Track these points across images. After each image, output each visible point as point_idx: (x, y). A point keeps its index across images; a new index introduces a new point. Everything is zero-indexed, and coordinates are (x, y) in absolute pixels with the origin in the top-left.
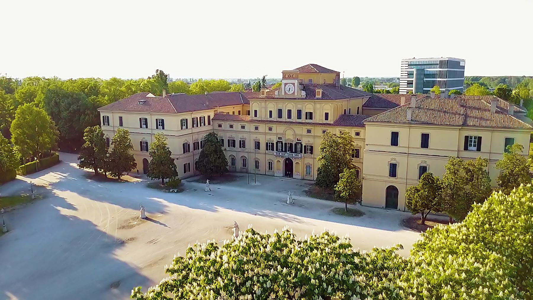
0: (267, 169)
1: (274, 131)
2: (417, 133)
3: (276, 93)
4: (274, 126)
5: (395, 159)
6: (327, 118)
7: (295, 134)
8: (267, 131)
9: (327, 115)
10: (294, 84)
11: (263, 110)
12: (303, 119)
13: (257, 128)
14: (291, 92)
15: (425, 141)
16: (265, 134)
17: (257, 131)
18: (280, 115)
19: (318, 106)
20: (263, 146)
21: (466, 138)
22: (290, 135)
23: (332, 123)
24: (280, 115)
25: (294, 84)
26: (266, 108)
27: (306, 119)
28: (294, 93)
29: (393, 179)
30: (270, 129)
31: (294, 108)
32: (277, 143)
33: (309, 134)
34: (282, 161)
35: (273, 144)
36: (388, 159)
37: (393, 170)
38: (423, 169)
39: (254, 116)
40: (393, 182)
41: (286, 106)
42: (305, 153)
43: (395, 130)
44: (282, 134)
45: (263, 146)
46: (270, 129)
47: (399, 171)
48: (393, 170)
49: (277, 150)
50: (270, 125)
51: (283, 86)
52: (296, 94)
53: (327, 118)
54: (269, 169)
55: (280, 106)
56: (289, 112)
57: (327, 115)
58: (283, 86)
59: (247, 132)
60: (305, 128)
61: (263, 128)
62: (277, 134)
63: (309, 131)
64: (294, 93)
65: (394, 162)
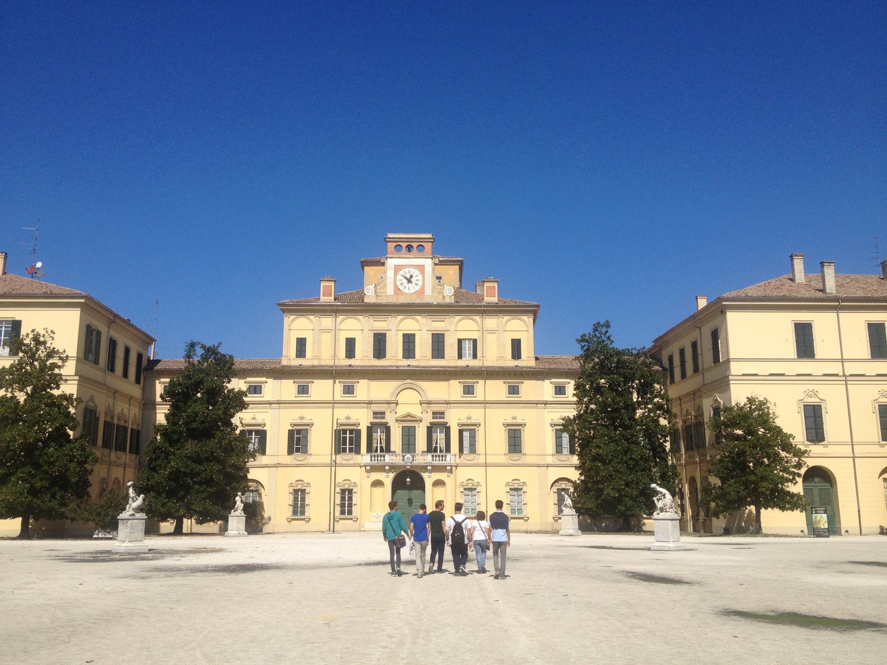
5: (815, 393)
6: (516, 351)
8: (339, 395)
9: (516, 345)
10: (421, 268)
11: (327, 338)
14: (412, 288)
16: (333, 403)
18: (380, 349)
19: (491, 322)
23: (532, 363)
24: (380, 349)
25: (421, 268)
26: (335, 331)
27: (460, 356)
28: (421, 292)
30: (349, 390)
32: (370, 430)
33: (469, 398)
34: (388, 479)
35: (359, 432)
43: (803, 317)
46: (349, 390)
49: (369, 449)
51: (390, 273)
52: (428, 291)
53: (516, 351)
56: (409, 341)
57: (516, 345)
58: (390, 273)
61: (321, 389)
62: (370, 403)
64: (421, 292)
65: (813, 400)
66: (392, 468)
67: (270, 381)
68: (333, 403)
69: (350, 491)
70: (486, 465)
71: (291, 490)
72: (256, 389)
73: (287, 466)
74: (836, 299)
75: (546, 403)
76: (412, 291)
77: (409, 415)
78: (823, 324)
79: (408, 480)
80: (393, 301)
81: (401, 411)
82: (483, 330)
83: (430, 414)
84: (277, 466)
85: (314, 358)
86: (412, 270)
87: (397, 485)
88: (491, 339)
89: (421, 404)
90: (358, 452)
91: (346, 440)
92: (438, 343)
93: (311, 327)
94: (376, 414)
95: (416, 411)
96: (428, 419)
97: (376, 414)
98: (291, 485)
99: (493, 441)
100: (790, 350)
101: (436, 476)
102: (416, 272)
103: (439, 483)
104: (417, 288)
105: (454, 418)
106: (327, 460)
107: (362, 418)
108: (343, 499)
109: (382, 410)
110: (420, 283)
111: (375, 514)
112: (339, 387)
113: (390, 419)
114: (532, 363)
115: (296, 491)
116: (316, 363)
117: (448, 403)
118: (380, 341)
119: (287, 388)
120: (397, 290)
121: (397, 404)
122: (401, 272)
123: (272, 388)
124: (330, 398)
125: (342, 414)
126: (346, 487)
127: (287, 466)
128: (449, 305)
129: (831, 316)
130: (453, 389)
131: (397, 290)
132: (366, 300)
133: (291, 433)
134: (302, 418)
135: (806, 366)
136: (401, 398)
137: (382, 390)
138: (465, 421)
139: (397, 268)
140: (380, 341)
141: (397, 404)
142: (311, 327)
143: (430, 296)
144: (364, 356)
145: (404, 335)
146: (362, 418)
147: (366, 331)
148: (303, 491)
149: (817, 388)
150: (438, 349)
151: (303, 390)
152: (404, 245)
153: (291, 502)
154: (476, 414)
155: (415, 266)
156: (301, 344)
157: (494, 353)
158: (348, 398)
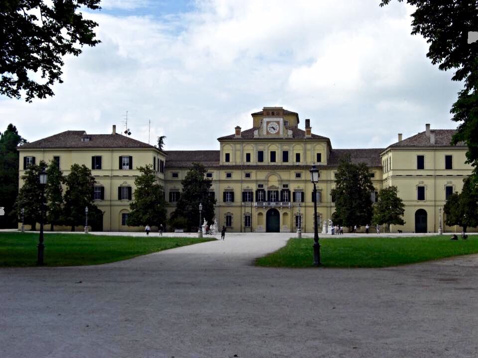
0: (243, 225)
1: (253, 177)
2: (441, 156)
3: (256, 133)
6: (319, 159)
7: (281, 181)
8: (244, 178)
9: (319, 156)
10: (278, 123)
13: (229, 175)
14: (274, 132)
17: (229, 179)
19: (309, 146)
20: (238, 197)
22: (274, 182)
23: (325, 164)
25: (278, 123)
26: (243, 150)
28: (278, 133)
29: (421, 203)
30: (248, 175)
31: (279, 150)
32: (257, 192)
33: (298, 179)
34: (265, 212)
36: (416, 182)
37: (421, 192)
38: (449, 190)
39: (225, 161)
40: (421, 205)
42: (294, 200)
43: (421, 153)
44: (264, 181)
45: (238, 197)
46: (248, 175)
47: (428, 194)
48: (421, 192)
49: (257, 201)
50: (248, 171)
52: (281, 133)
54: (246, 225)
55: (261, 148)
57: (319, 156)
59: (215, 181)
61: (237, 175)
62: (257, 181)
63: (298, 175)
64: (278, 133)
65: (422, 185)
66: (266, 207)
67: (215, 171)
68: (242, 181)
69: (249, 217)
70: (305, 207)
71: (225, 216)
72: (210, 175)
73: (224, 206)
74: (433, 146)
75: (331, 181)
76: (274, 132)
77: (273, 186)
79: (273, 213)
80: (267, 137)
81: (270, 184)
82: (305, 150)
83: (282, 186)
84: (220, 206)
85: (232, 162)
86: (274, 123)
87: (268, 214)
88: (309, 153)
89: (279, 181)
90: (252, 200)
91: (247, 196)
92: (285, 156)
93: (231, 149)
94: (259, 186)
95: (276, 184)
96: (280, 188)
97: (259, 186)
98: (225, 214)
100: (415, 166)
101: (285, 211)
102: (275, 125)
103: (285, 214)
104: (277, 131)
105: (292, 187)
106: (239, 204)
107: (254, 187)
108: (246, 220)
109: (262, 184)
110: (278, 129)
111: (259, 226)
112: (244, 175)
113: (266, 188)
114: (325, 164)
115: (227, 217)
116: (234, 164)
117: (289, 181)
118: (261, 156)
119: (222, 175)
120: (268, 133)
121: (268, 181)
122: (270, 124)
123: (217, 175)
124: (240, 179)
126: (248, 215)
127: (224, 206)
128: (290, 139)
130: (292, 175)
131: (268, 133)
132: (255, 137)
133: (224, 193)
134: (229, 187)
135: (420, 172)
136: (270, 179)
137: (261, 175)
138: (297, 189)
139: (268, 123)
140: (261, 156)
141: (268, 181)
142: (231, 149)
143: (282, 135)
145: (271, 152)
146: (254, 187)
147: (255, 150)
148: (230, 217)
149: (423, 180)
151: (229, 175)
152: (271, 112)
153: (225, 221)
154: (302, 186)
155: (275, 122)
156: (228, 156)
157: (311, 160)
158: (248, 179)
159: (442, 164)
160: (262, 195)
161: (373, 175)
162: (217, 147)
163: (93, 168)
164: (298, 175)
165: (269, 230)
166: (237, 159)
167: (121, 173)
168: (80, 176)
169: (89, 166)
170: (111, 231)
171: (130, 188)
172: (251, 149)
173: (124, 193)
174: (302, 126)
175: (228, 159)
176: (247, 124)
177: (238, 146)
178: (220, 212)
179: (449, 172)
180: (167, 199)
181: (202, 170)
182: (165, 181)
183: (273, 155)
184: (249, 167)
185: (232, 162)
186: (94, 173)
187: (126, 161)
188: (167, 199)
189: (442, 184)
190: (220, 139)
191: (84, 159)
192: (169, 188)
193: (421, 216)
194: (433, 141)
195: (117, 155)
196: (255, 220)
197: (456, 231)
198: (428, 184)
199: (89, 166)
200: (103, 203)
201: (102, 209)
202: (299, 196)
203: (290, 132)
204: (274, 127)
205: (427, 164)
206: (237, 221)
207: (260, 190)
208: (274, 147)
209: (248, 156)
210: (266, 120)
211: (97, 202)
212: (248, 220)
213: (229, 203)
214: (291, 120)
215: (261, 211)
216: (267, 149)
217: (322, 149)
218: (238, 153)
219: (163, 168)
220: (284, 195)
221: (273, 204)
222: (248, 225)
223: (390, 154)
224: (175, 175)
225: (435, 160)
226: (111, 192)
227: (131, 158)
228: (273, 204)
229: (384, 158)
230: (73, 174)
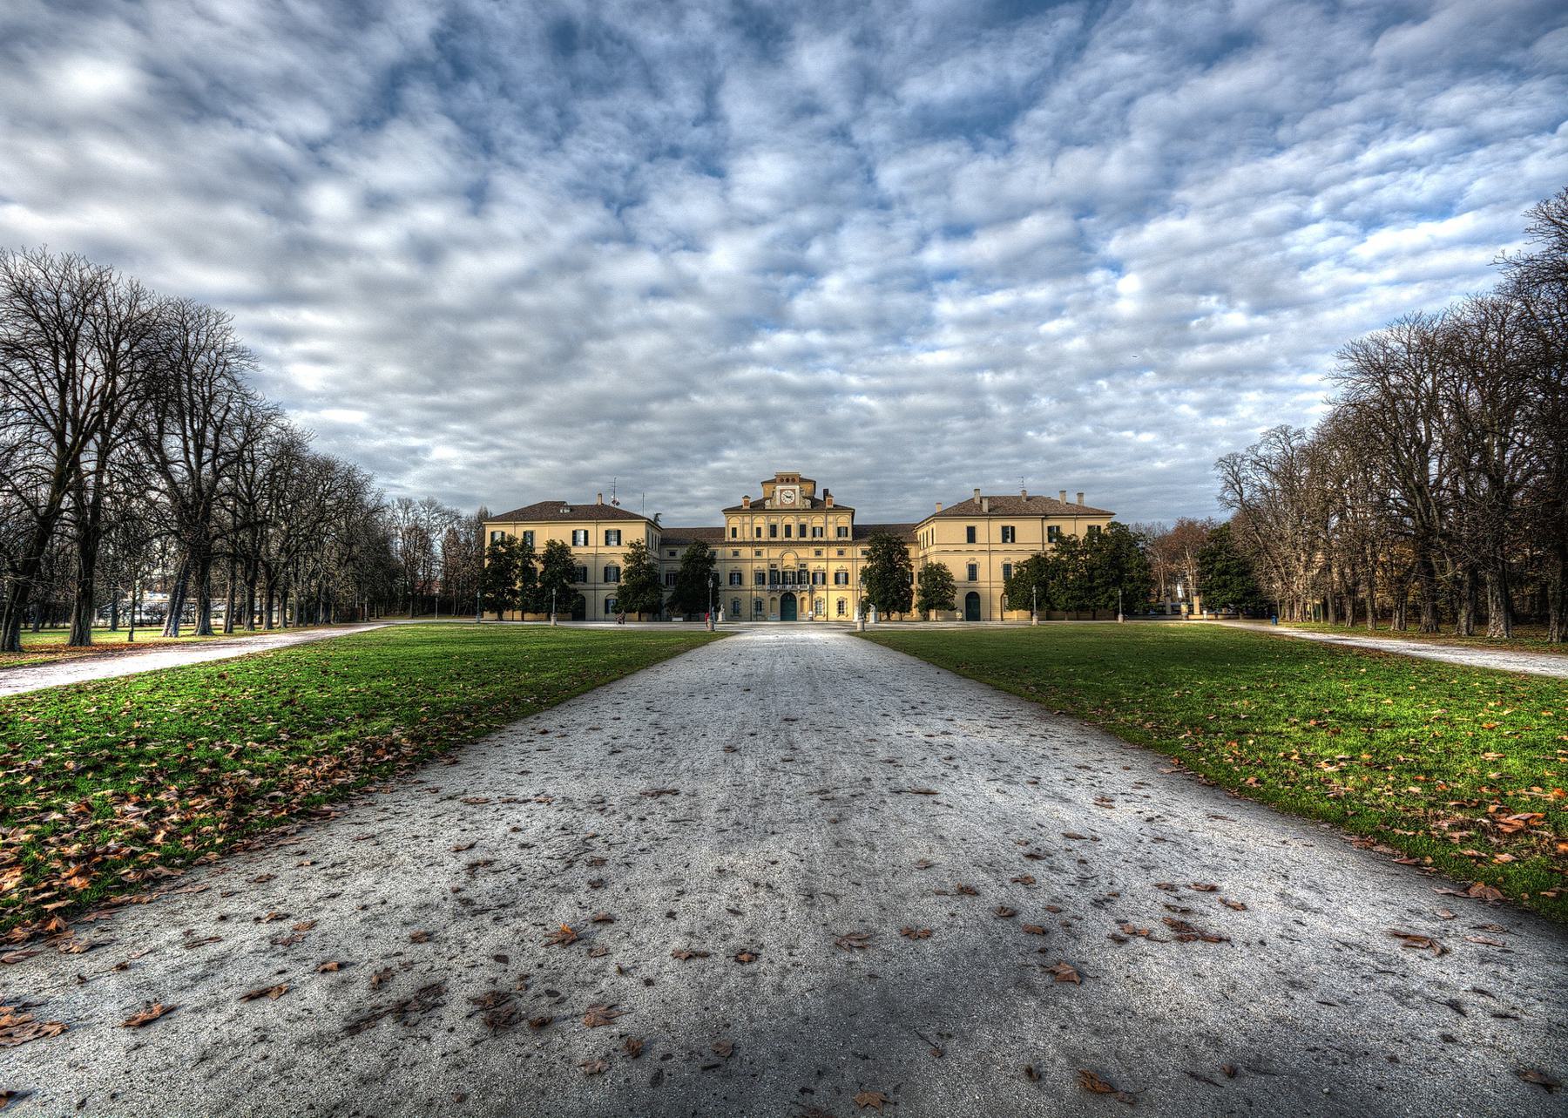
1: (765, 556)
3: (768, 503)
4: (765, 550)
12: (808, 538)
14: (789, 501)
15: (1008, 534)
18: (774, 534)
19: (831, 518)
21: (1050, 529)
22: (788, 561)
24: (774, 534)
30: (758, 553)
37: (973, 569)
38: (1007, 568)
41: (781, 521)
43: (971, 524)
46: (758, 553)
47: (982, 574)
48: (973, 569)
55: (774, 520)
60: (812, 550)
61: (746, 552)
63: (818, 553)
78: (981, 527)
92: (803, 529)
95: (793, 564)
99: (831, 579)
105: (812, 567)
125: (756, 566)
129: (985, 523)
137: (775, 553)
144: (765, 536)
146: (764, 566)
150: (803, 534)
154: (823, 565)
159: (997, 536)
160: (774, 577)
161: (907, 552)
162: (720, 522)
163: (574, 543)
164: (818, 553)
165: (783, 619)
166: (746, 534)
167: (607, 550)
168: (557, 553)
169: (569, 542)
170: (595, 620)
171: (618, 569)
172: (761, 521)
173: (610, 573)
174: (819, 495)
175: (734, 535)
176: (758, 494)
177: (747, 519)
178: (727, 595)
179: (1008, 546)
180: (663, 581)
181: (705, 546)
182: (661, 560)
183: (788, 528)
184: (760, 544)
185: (739, 538)
186: (574, 551)
187: (613, 537)
188: (663, 581)
189: (998, 561)
190: (726, 511)
191: (560, 533)
192: (664, 569)
193: (973, 600)
194: (985, 508)
195: (603, 528)
196: (767, 605)
197: (1015, 616)
198: (982, 560)
199: (569, 542)
200: (586, 586)
201: (584, 593)
202: (819, 577)
203: (808, 502)
204: (789, 495)
205: (981, 535)
206: (746, 607)
207: (773, 572)
208: (790, 520)
209: (759, 530)
210: (779, 487)
211: (579, 586)
212: (759, 605)
213: (736, 586)
214: (809, 487)
215: (774, 595)
216: (781, 521)
217: (844, 521)
218: (747, 527)
219: (665, 542)
220: (801, 576)
221: (788, 587)
222: (759, 612)
223: (933, 525)
224: (673, 554)
225: (989, 531)
226: (596, 575)
227: (619, 532)
228: (788, 587)
229: (920, 533)
230: (549, 552)
